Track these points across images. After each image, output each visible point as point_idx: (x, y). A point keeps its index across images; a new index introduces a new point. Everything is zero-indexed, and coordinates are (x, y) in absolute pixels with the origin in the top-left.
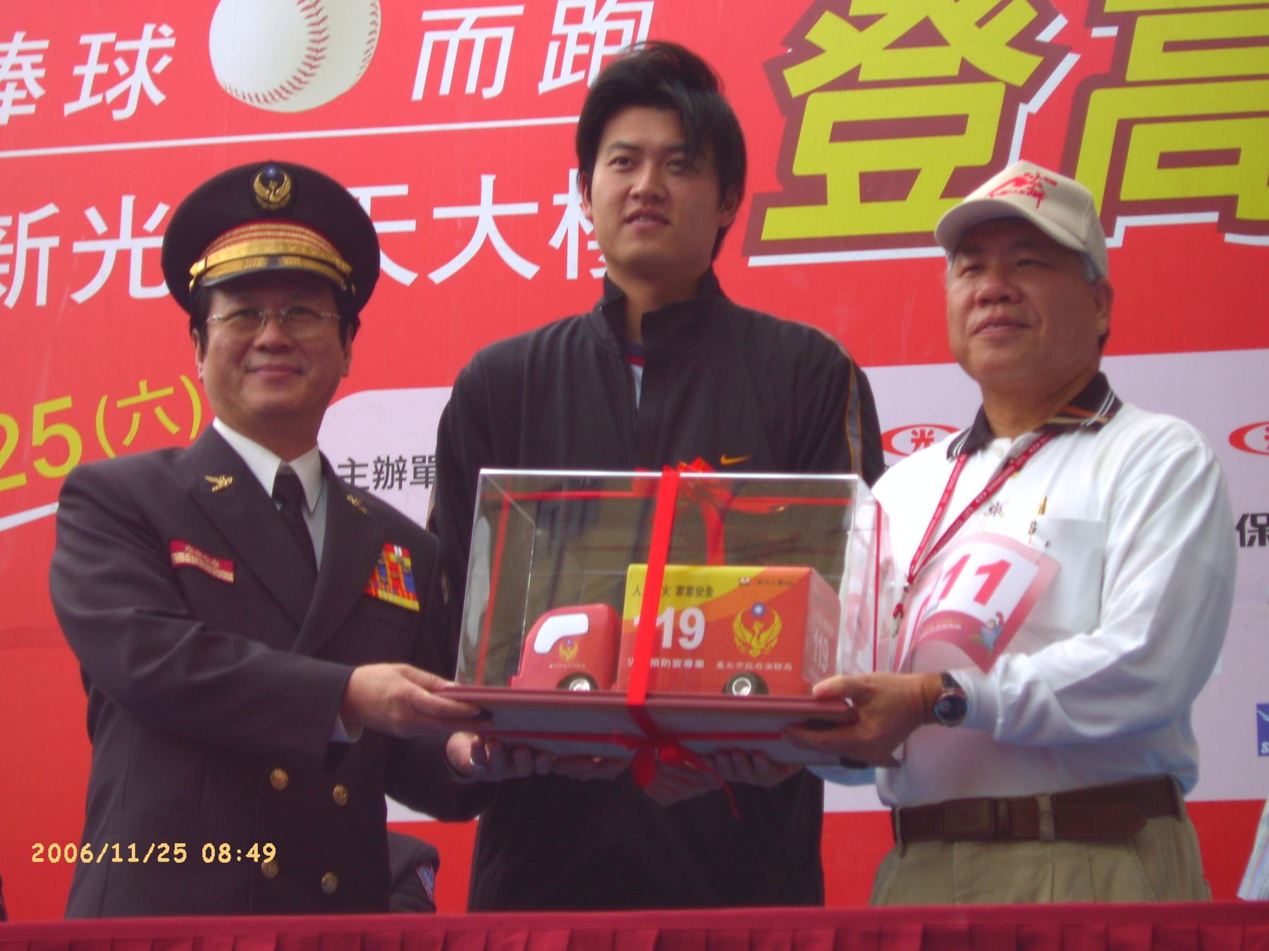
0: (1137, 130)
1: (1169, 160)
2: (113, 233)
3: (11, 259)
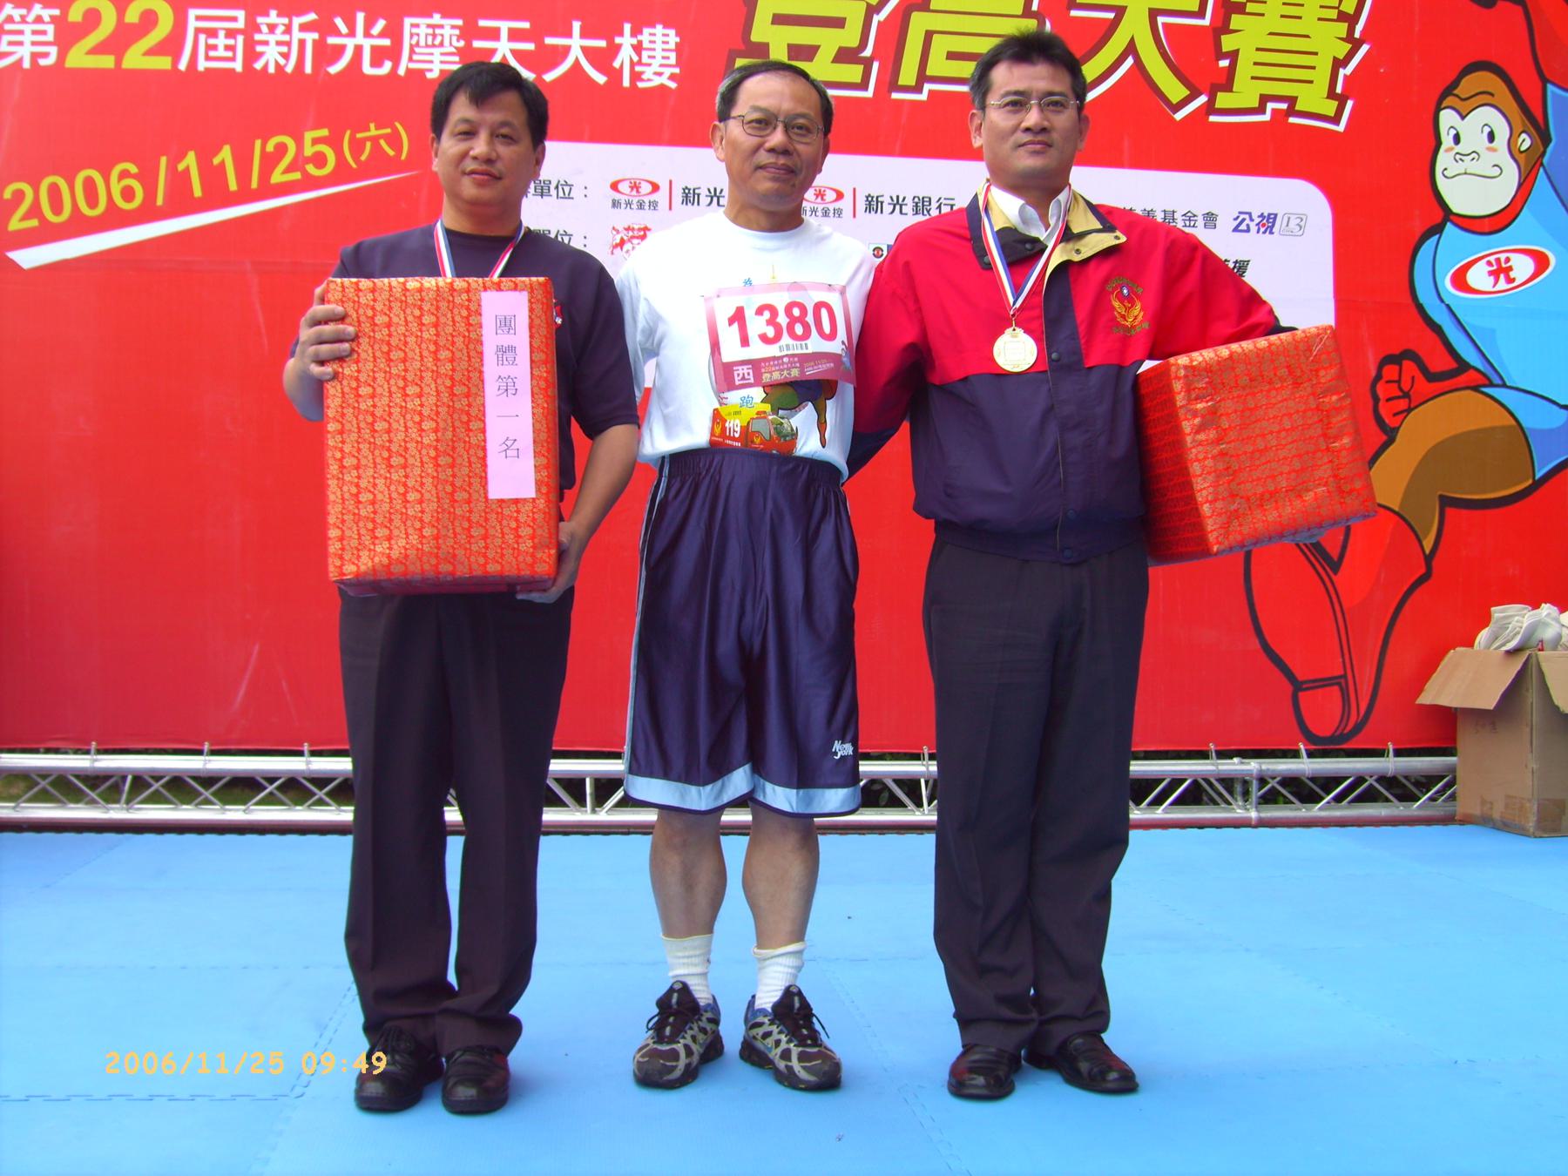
1: (952, 56)
2: (352, 34)
3: (288, 44)
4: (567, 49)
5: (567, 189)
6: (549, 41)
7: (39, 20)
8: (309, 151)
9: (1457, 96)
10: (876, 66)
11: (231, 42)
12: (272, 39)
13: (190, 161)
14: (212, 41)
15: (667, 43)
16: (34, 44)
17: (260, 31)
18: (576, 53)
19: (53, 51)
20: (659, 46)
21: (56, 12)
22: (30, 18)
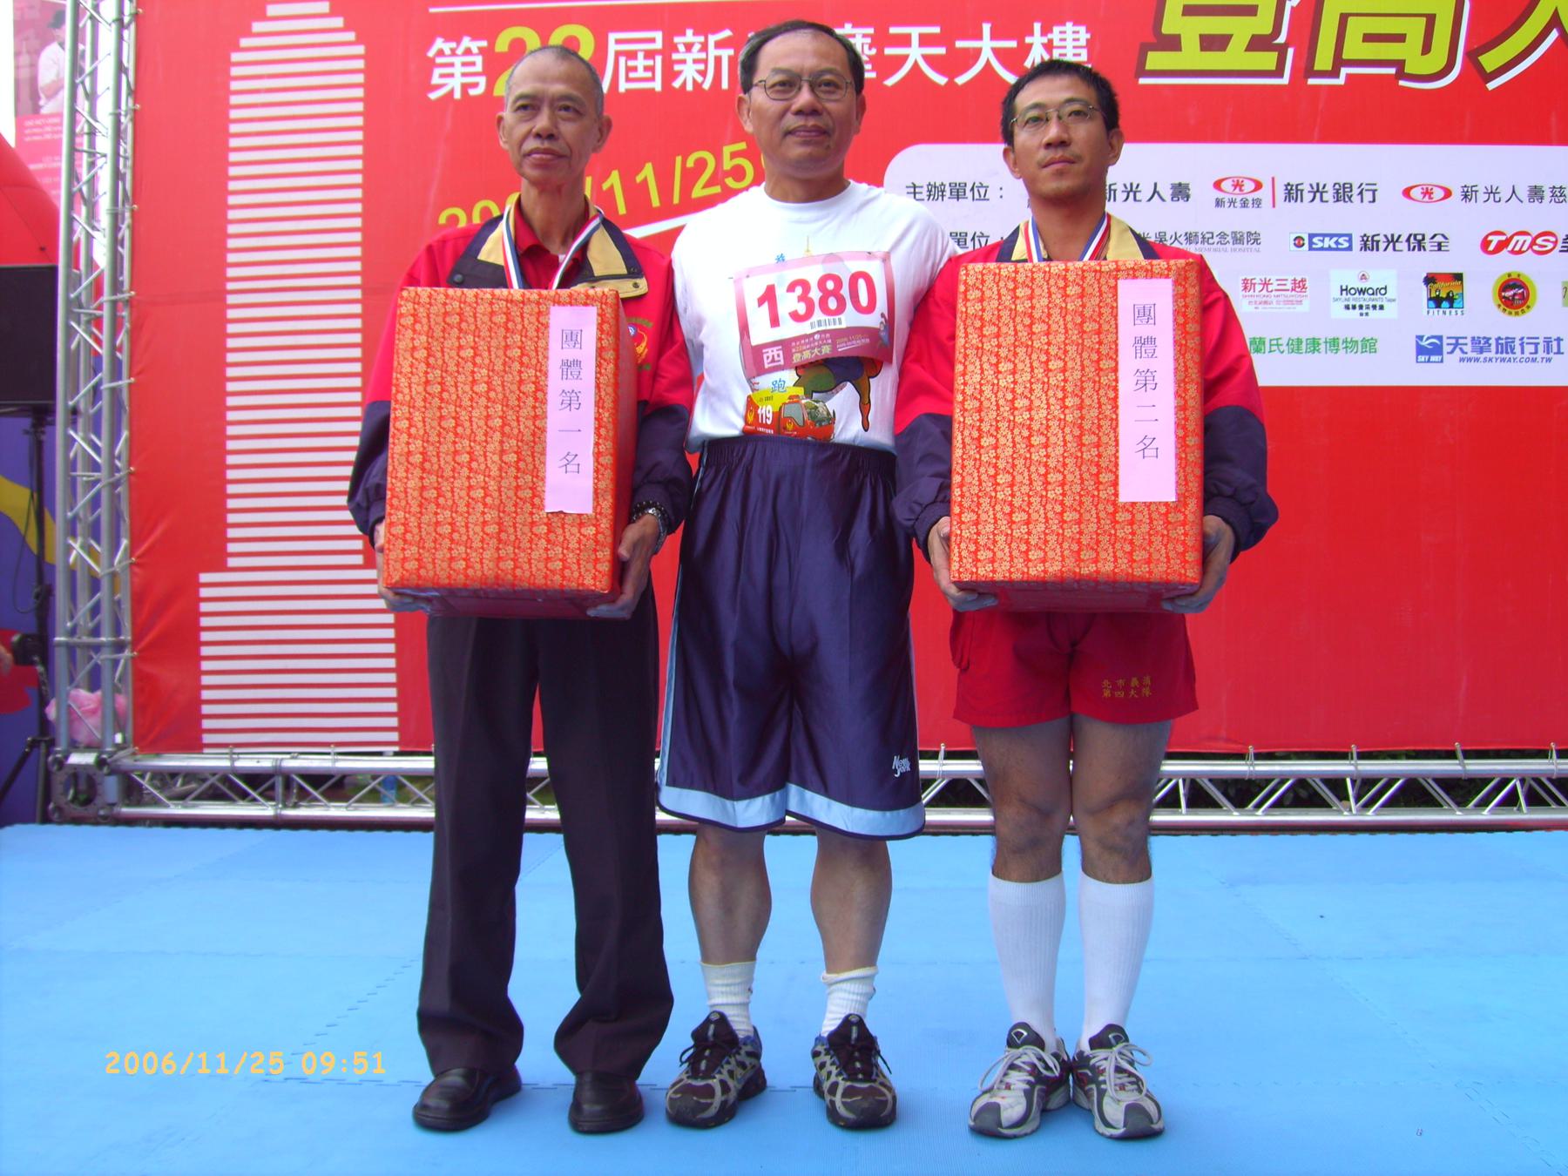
0: (1351, 20)
1: (1369, 38)
3: (705, 62)
4: (978, 51)
5: (982, 191)
6: (960, 44)
7: (468, 52)
8: (728, 164)
10: (1291, 51)
11: (650, 63)
12: (689, 57)
13: (614, 180)
14: (631, 63)
15: (1077, 40)
16: (464, 75)
17: (677, 51)
18: (987, 55)
19: (482, 81)
20: (1069, 44)
21: (484, 44)
22: (460, 51)
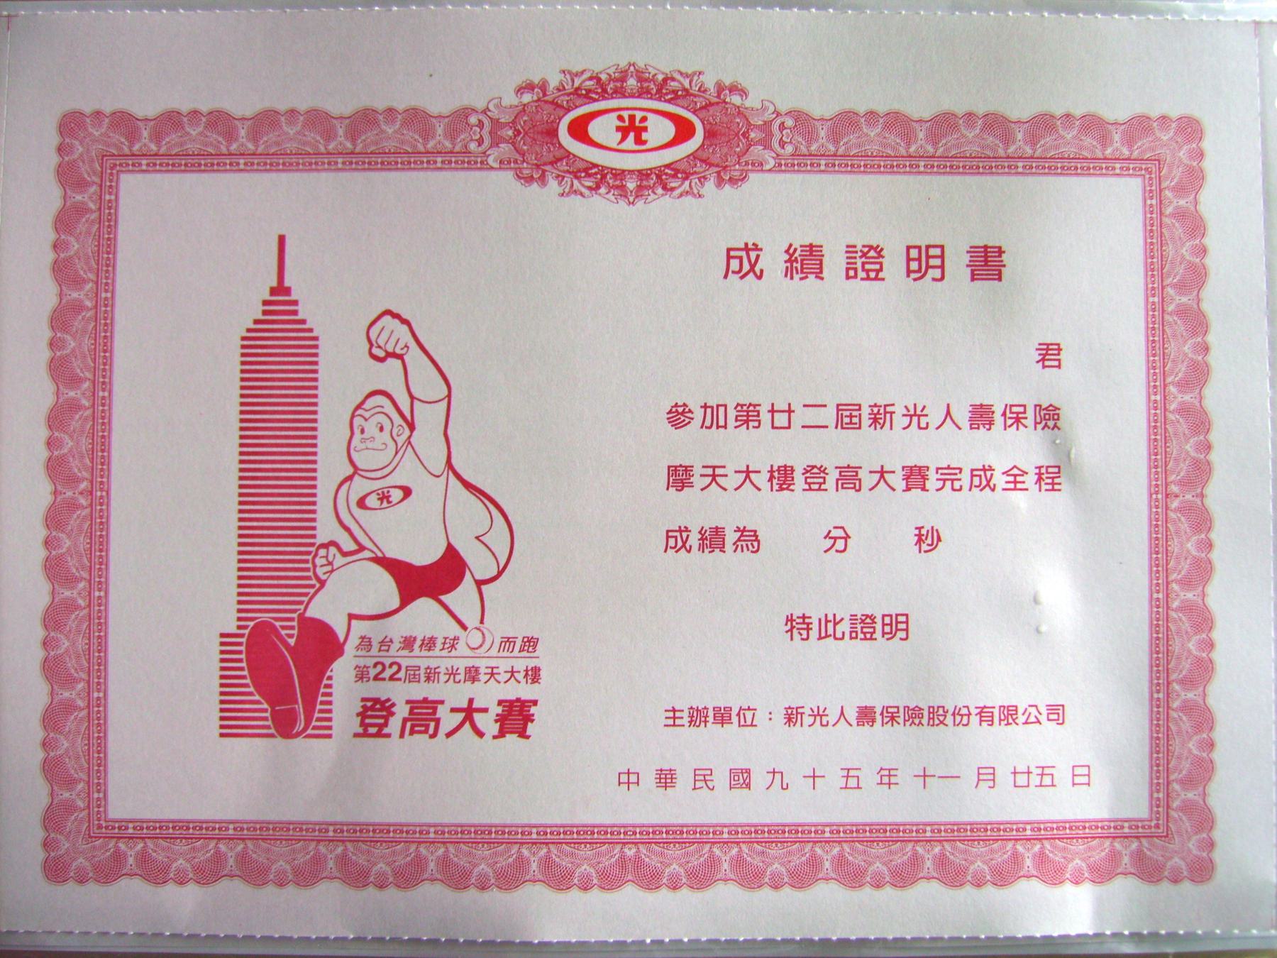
9: (364, 409)
